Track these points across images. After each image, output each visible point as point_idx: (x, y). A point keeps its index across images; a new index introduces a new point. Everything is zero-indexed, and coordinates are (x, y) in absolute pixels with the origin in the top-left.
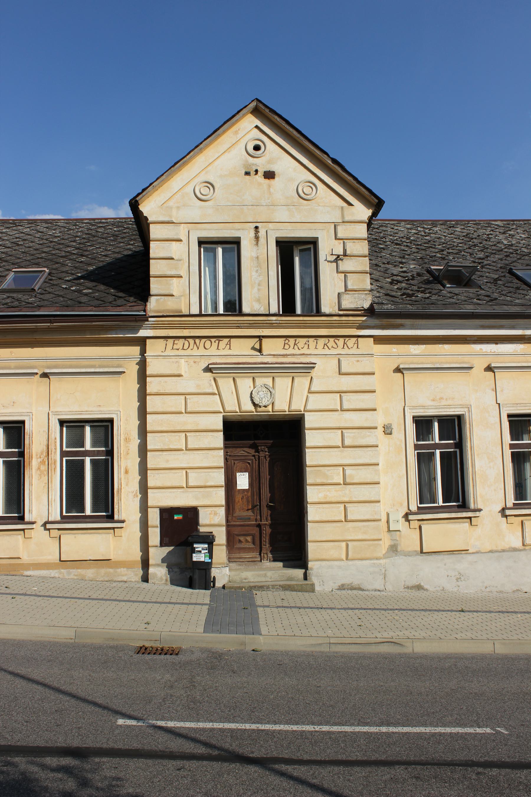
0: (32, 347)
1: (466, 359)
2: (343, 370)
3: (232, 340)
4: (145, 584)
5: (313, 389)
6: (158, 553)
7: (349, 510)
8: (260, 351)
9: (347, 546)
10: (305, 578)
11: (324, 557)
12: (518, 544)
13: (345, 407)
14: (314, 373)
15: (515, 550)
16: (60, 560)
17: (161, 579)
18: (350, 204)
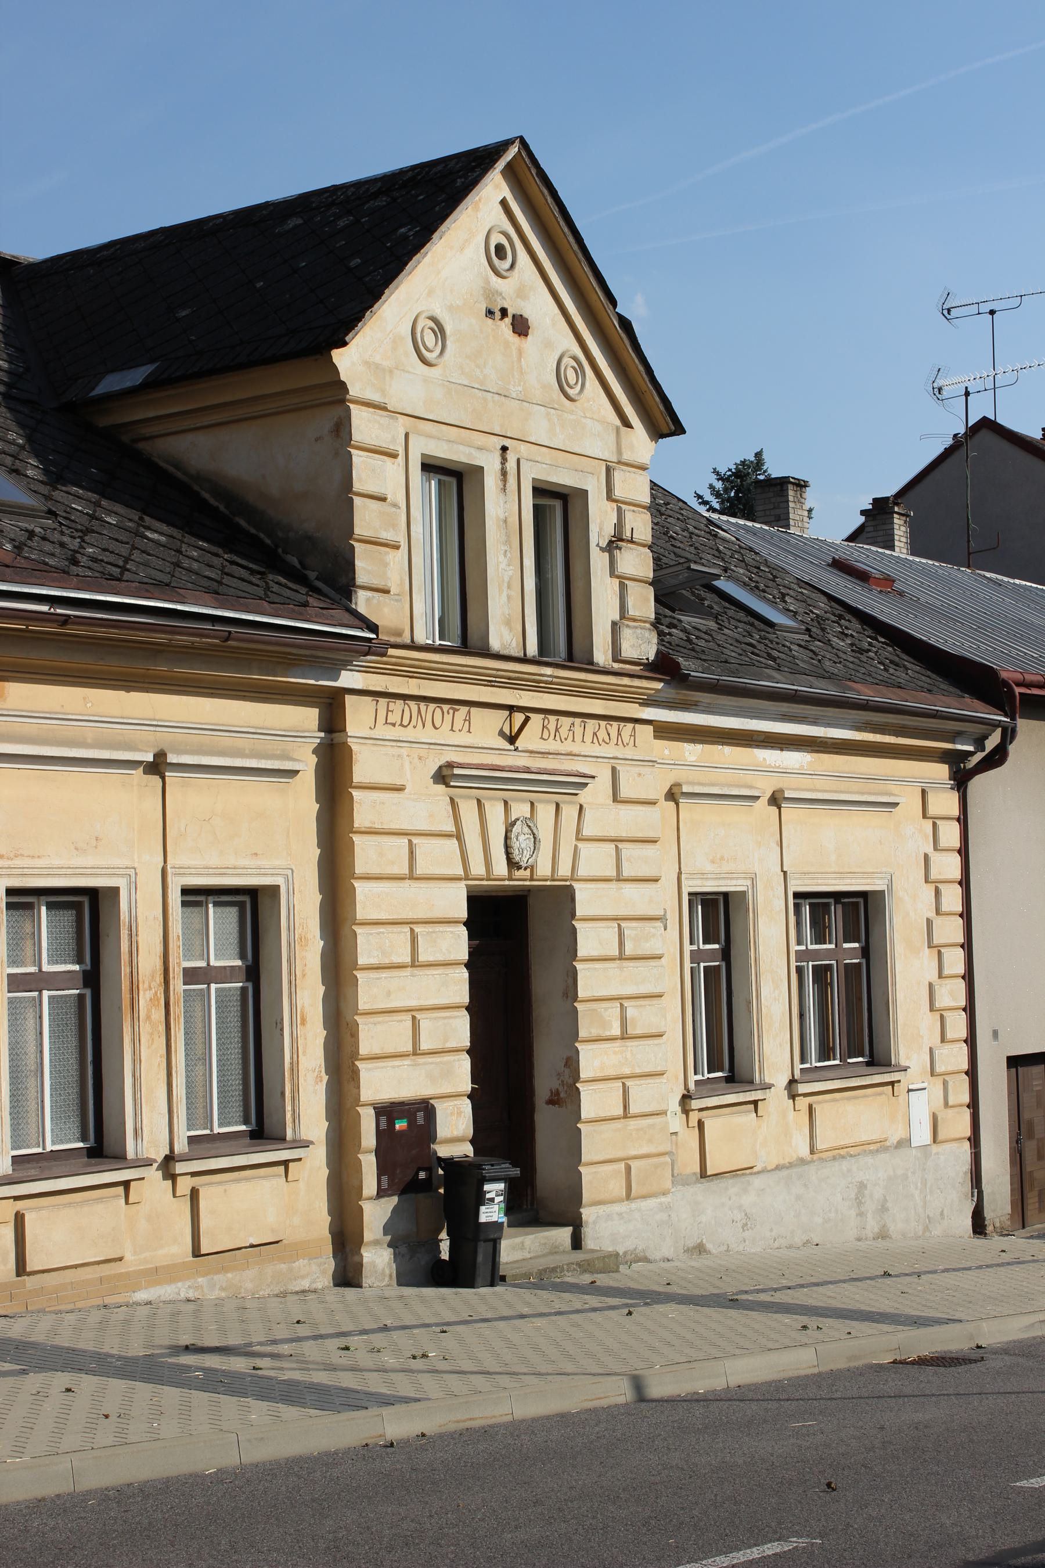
0: (128, 689)
1: (749, 777)
2: (625, 792)
3: (474, 710)
4: (350, 1293)
5: (586, 832)
6: (376, 1213)
7: (632, 1092)
8: (512, 739)
9: (628, 1169)
10: (577, 1243)
11: (603, 1197)
12: (804, 1151)
13: (626, 873)
14: (584, 796)
15: (802, 1162)
16: (196, 1253)
17: (383, 1273)
18: (627, 424)
